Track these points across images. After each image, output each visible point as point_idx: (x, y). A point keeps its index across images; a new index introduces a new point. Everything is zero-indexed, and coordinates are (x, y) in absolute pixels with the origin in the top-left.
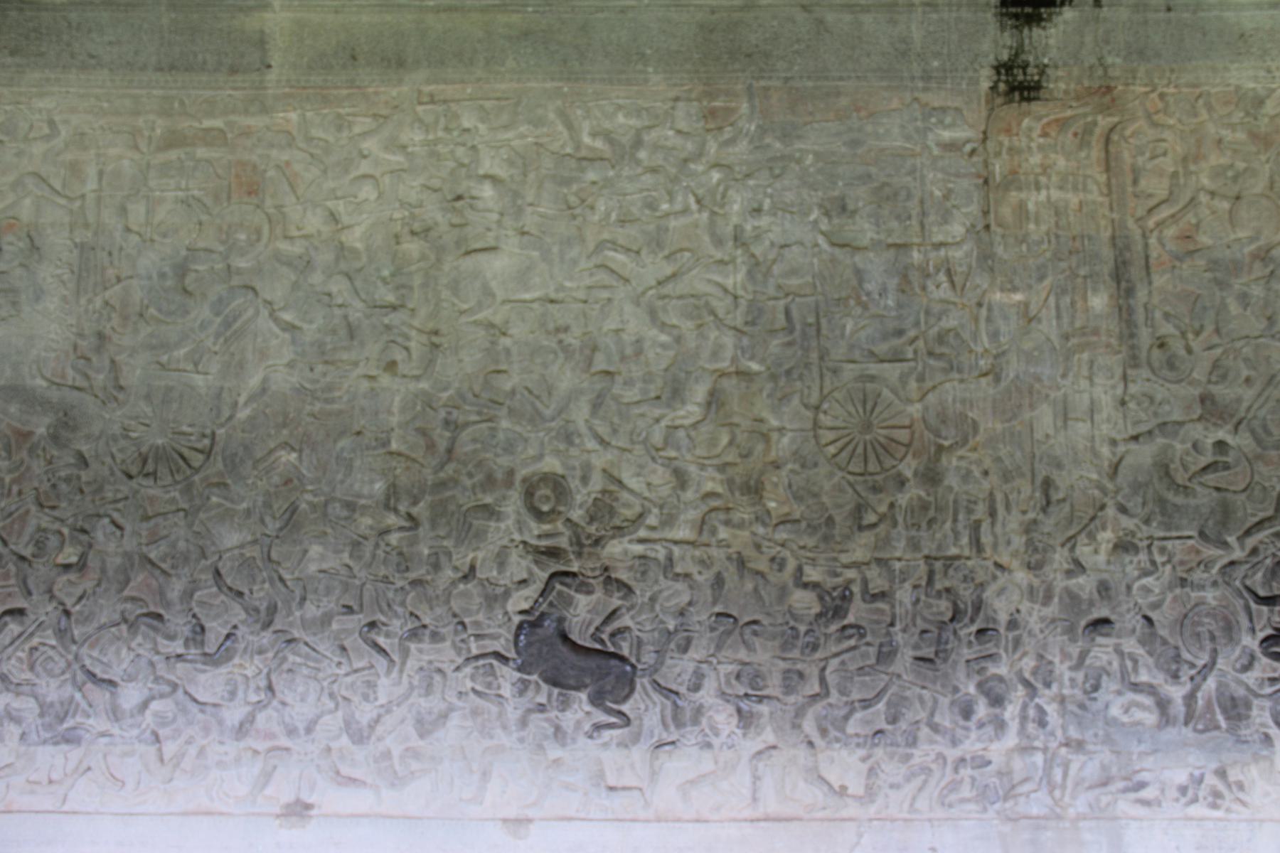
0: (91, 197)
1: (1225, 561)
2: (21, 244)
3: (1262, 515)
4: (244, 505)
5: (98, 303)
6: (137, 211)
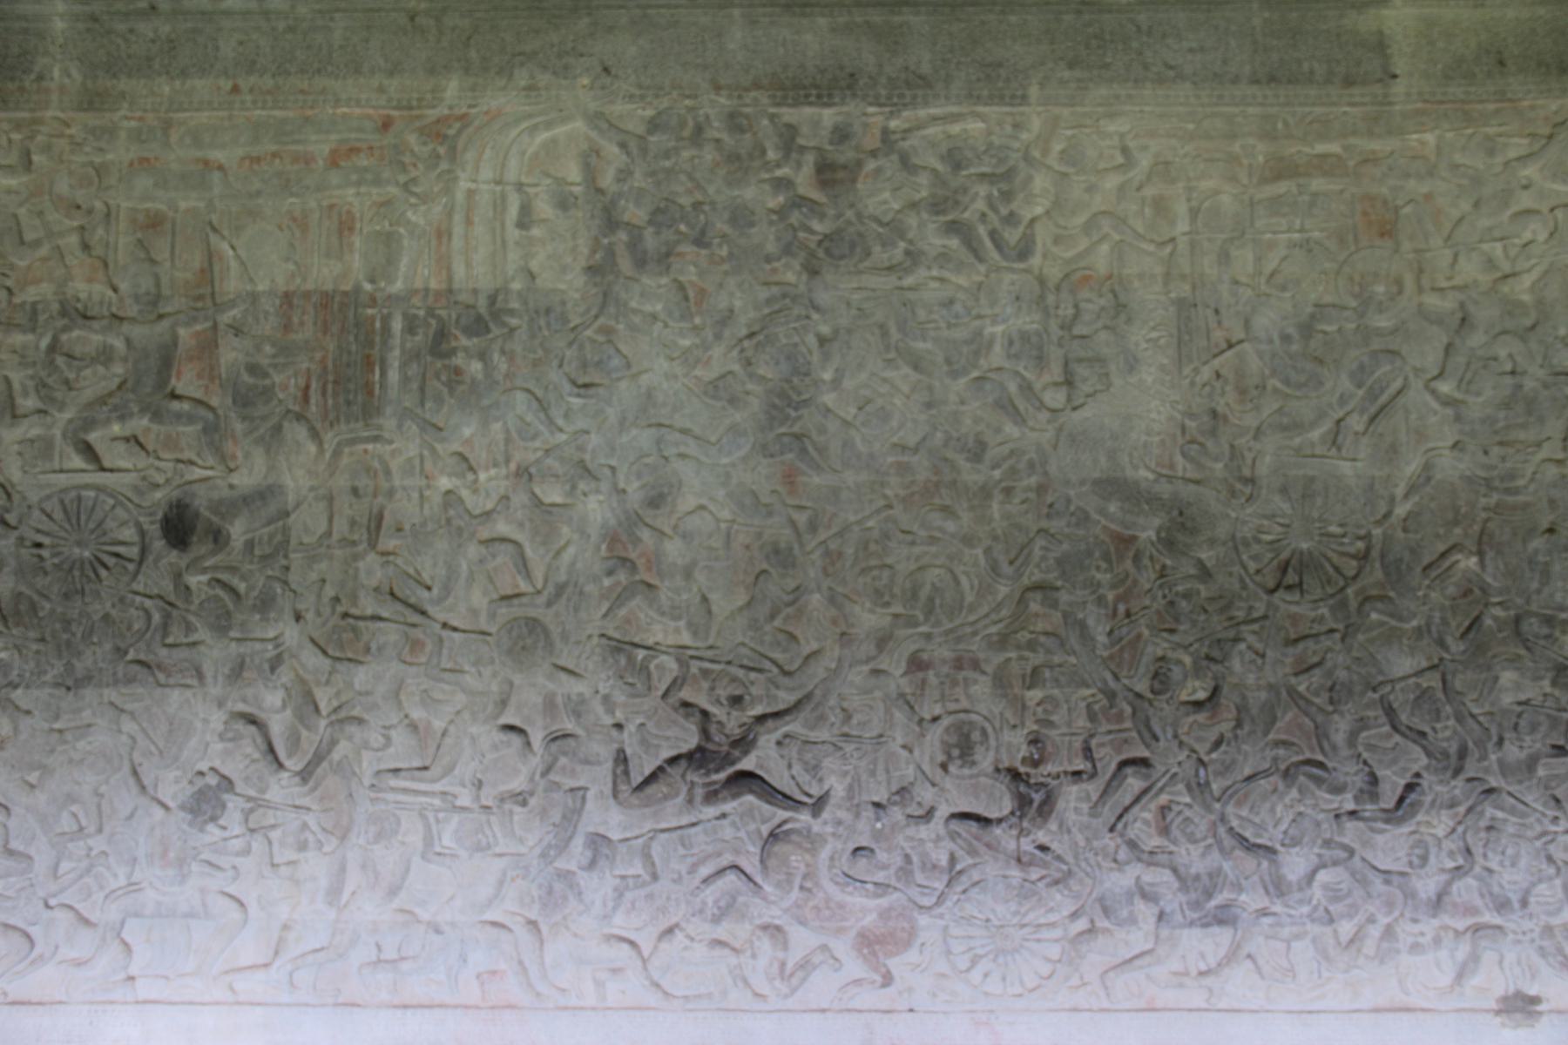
0: (1183, 244)
2: (1102, 302)
4: (1414, 623)
5: (1206, 373)
6: (1244, 259)
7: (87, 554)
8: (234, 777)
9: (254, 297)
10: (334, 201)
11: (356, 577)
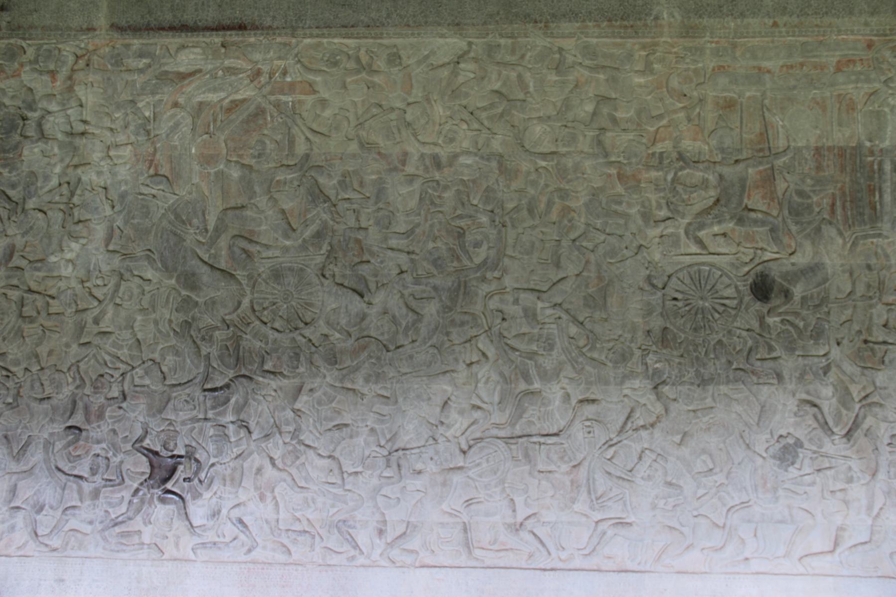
7: (707, 304)
8: (802, 438)
9: (798, 150)
10: (842, 92)
11: (871, 318)
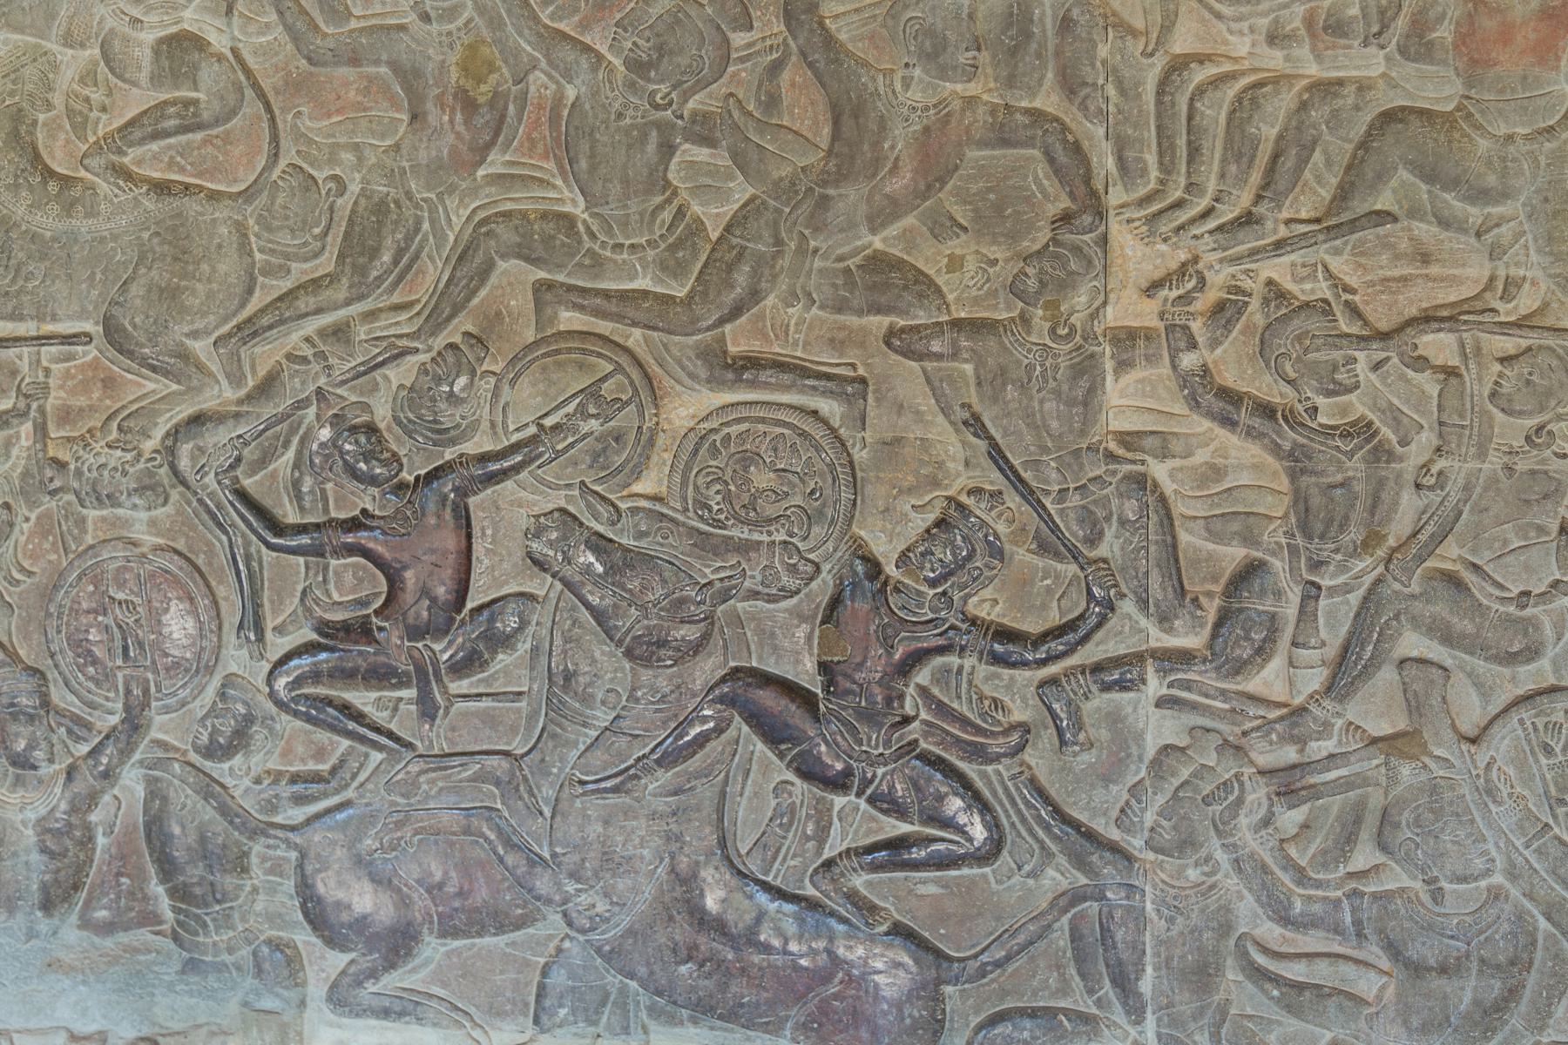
1: (184, 411)
3: (300, 271)
